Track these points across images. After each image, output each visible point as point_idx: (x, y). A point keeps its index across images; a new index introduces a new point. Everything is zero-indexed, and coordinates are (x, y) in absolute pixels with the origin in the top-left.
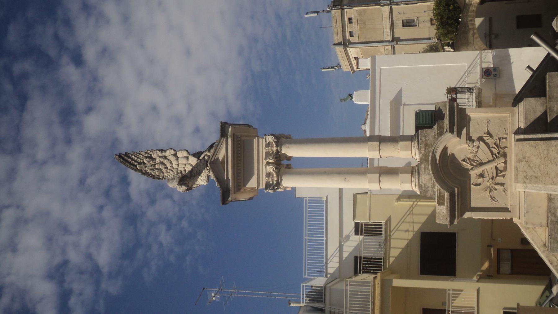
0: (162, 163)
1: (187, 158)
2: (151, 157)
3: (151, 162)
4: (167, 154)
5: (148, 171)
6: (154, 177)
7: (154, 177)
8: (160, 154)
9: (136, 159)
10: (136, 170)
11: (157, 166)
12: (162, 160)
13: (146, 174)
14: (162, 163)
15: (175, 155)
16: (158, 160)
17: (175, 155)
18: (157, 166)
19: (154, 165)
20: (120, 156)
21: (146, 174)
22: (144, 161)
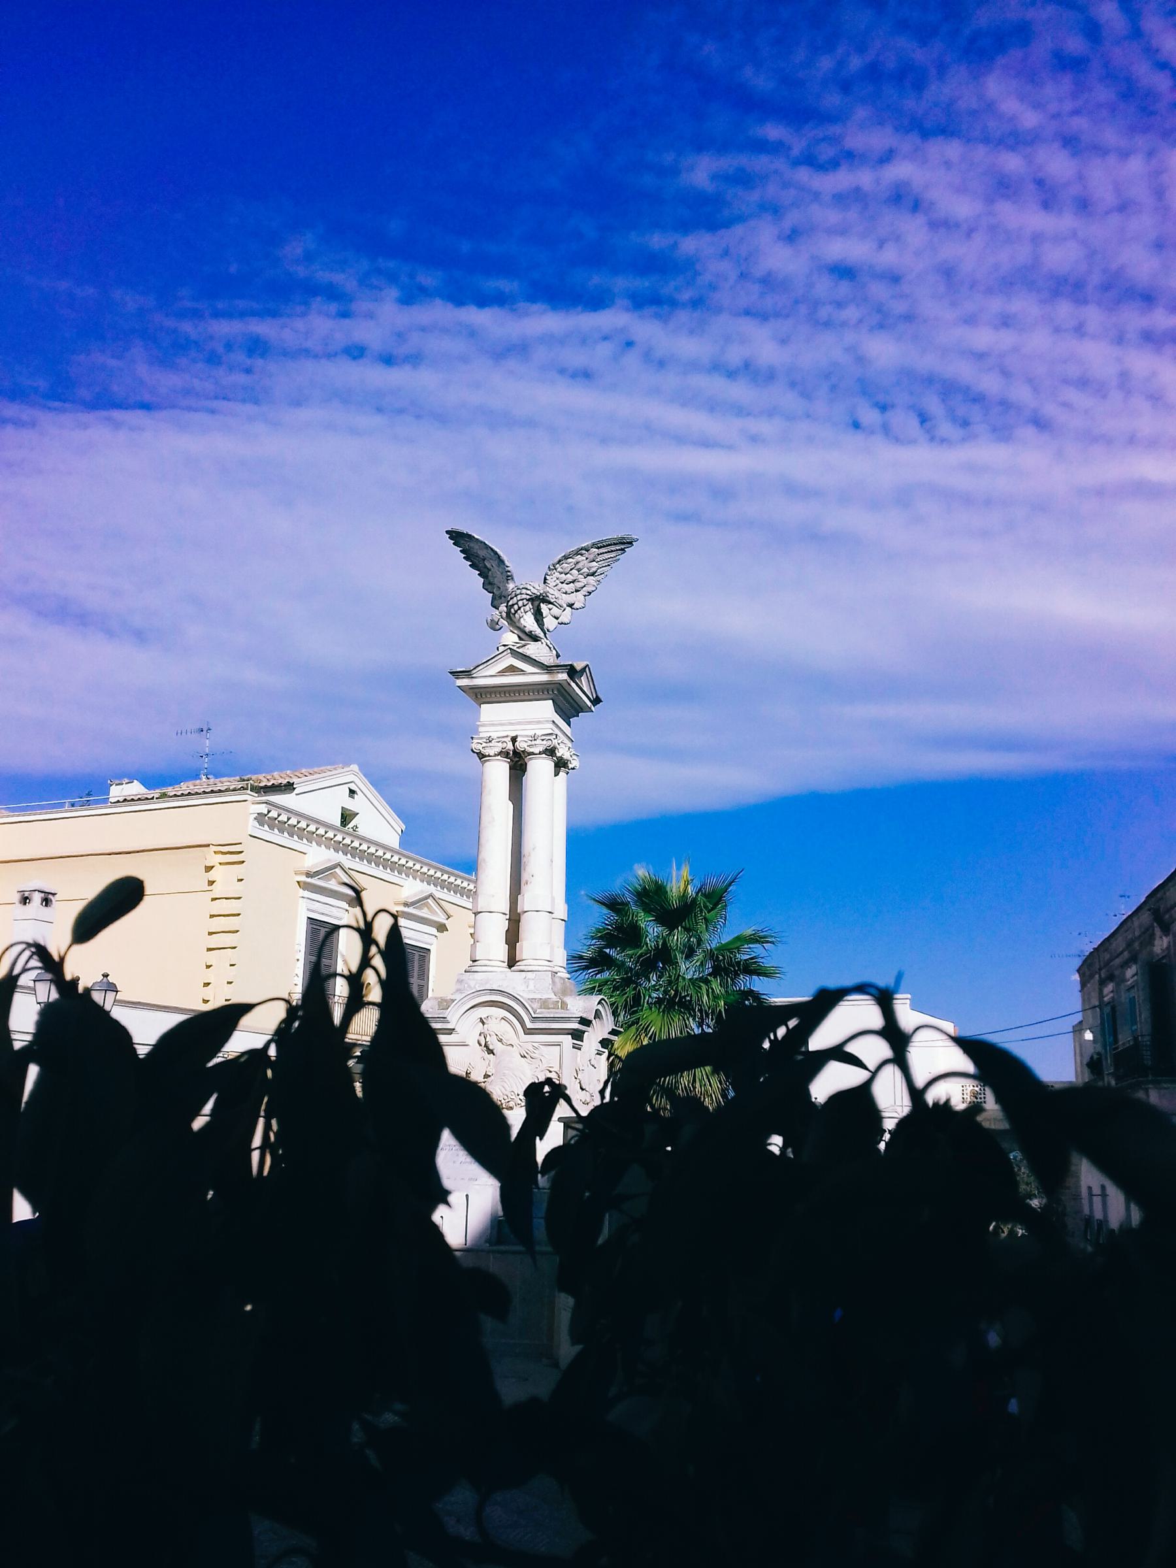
0: (573, 582)
2: (593, 574)
3: (585, 570)
4: (580, 595)
5: (579, 558)
6: (566, 557)
7: (566, 557)
8: (590, 589)
9: (607, 556)
10: (594, 545)
11: (574, 572)
12: (578, 585)
13: (578, 553)
14: (573, 582)
15: (571, 605)
16: (584, 581)
17: (571, 605)
18: (574, 572)
19: (579, 570)
20: (631, 543)
21: (578, 553)
22: (594, 564)
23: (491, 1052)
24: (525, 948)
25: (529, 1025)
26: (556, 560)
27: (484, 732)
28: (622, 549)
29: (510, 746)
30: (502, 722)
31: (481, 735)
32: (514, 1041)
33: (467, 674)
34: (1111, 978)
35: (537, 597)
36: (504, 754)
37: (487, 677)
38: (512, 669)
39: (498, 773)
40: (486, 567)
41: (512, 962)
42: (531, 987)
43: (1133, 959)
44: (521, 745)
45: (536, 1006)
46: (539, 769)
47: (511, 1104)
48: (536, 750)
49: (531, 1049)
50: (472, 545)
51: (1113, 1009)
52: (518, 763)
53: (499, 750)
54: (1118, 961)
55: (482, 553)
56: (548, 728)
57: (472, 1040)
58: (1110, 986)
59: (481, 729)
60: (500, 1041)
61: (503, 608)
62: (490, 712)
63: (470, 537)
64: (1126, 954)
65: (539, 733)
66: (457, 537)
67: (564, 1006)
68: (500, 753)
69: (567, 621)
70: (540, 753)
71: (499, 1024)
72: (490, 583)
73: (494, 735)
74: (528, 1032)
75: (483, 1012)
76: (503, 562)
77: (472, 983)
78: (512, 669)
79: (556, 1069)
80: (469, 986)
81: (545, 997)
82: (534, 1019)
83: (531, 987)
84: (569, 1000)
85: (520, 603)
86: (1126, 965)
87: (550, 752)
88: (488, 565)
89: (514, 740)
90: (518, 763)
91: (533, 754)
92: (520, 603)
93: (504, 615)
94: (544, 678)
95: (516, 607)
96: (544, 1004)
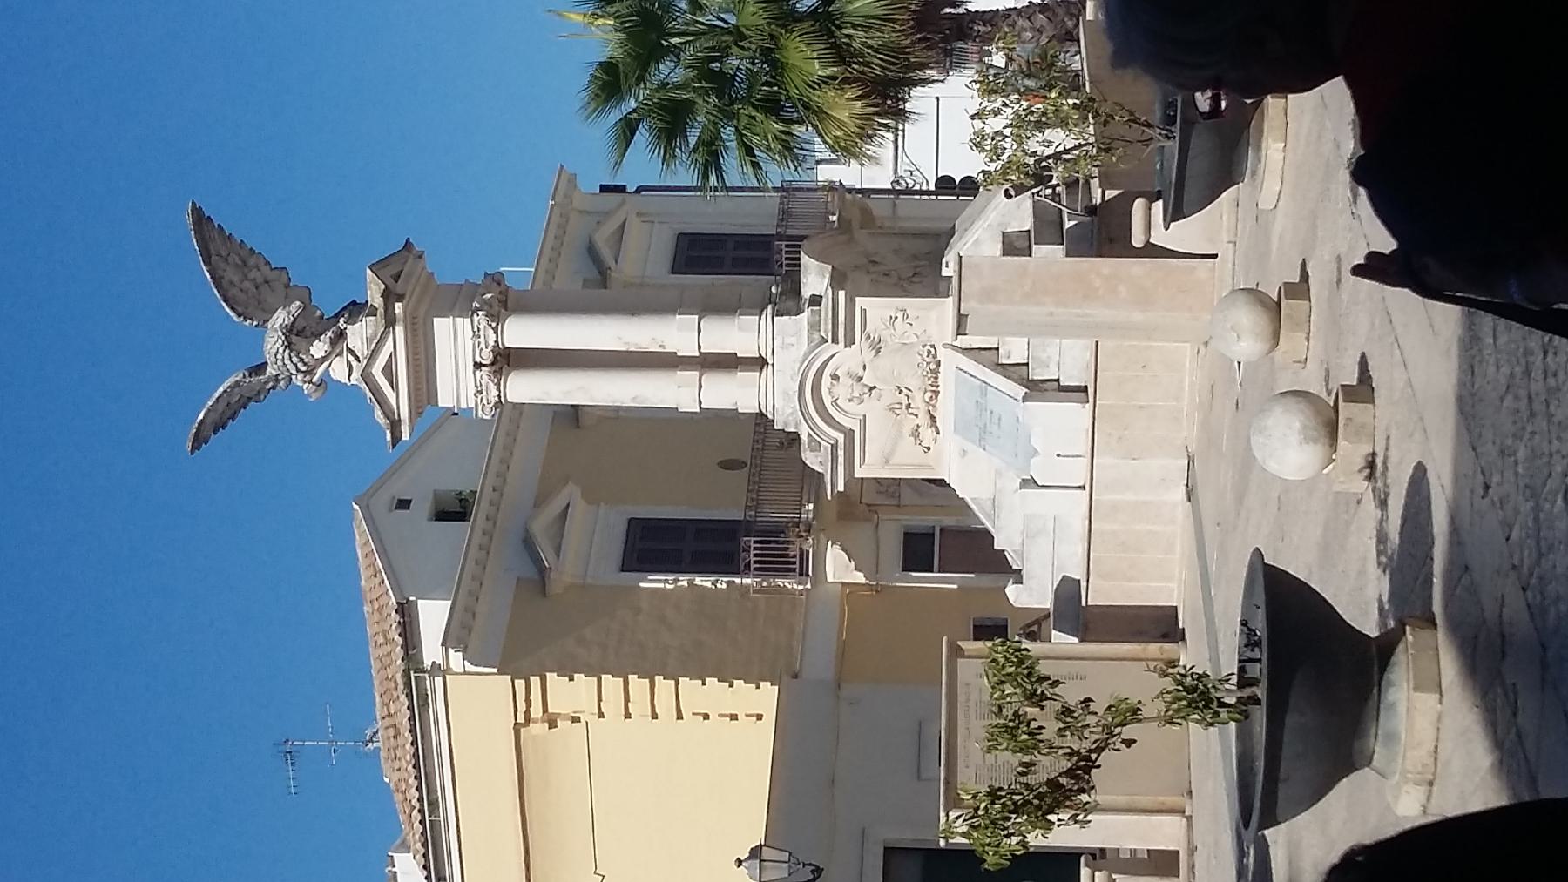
10: (207, 262)
24: (746, 350)
27: (468, 401)
31: (472, 405)
33: (395, 425)
38: (389, 371)
42: (792, 340)
44: (487, 357)
45: (816, 336)
48: (492, 337)
52: (506, 360)
59: (464, 406)
62: (445, 399)
78: (389, 371)
83: (792, 340)
84: (807, 292)
89: (478, 366)
90: (506, 360)
92: (295, 359)
93: (308, 378)
94: (400, 329)
96: (814, 326)
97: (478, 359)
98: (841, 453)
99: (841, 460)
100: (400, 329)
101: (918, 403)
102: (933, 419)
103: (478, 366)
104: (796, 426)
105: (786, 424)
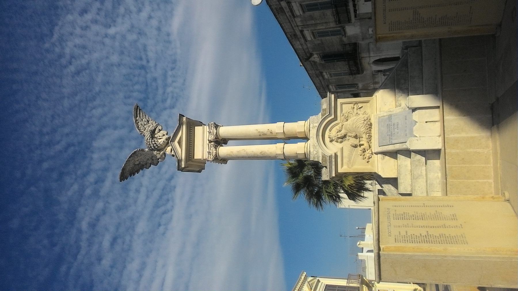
1: (164, 135)
2: (148, 121)
7: (138, 127)
9: (141, 115)
17: (160, 130)
19: (145, 125)
20: (138, 107)
21: (137, 124)
23: (345, 136)
25: (333, 117)
26: (138, 131)
27: (206, 156)
28: (140, 110)
29: (212, 143)
30: (202, 150)
32: (340, 125)
33: (179, 161)
34: (328, 86)
35: (151, 135)
36: (216, 147)
37: (182, 152)
38: (180, 143)
39: (223, 151)
40: (138, 164)
41: (306, 139)
43: (321, 73)
44: (212, 138)
46: (224, 131)
47: (369, 123)
49: (343, 117)
50: (127, 169)
51: (337, 85)
53: (214, 149)
54: (323, 83)
55: (131, 165)
56: (206, 128)
57: (339, 145)
58: (331, 87)
59: (205, 158)
60: (340, 131)
61: (155, 153)
63: (123, 169)
64: (321, 78)
65: (208, 130)
66: (123, 177)
67: (325, 110)
68: (216, 149)
69: (166, 132)
70: (216, 130)
71: (333, 132)
72: (146, 164)
73: (208, 150)
74: (335, 118)
75: (327, 140)
76: (135, 152)
77: (315, 152)
78: (180, 143)
79: (352, 105)
80: (316, 154)
81: (321, 117)
82: (330, 114)
85: (153, 143)
86: (323, 77)
87: (217, 126)
88: (137, 163)
89: (210, 142)
91: (217, 133)
92: (153, 143)
93: (158, 152)
94: (184, 127)
95: (155, 145)
96: (322, 115)
97: (210, 139)
98: (333, 160)
99: (334, 163)
100: (184, 127)
101: (364, 141)
102: (370, 147)
103: (210, 142)
104: (318, 159)
105: (314, 158)
